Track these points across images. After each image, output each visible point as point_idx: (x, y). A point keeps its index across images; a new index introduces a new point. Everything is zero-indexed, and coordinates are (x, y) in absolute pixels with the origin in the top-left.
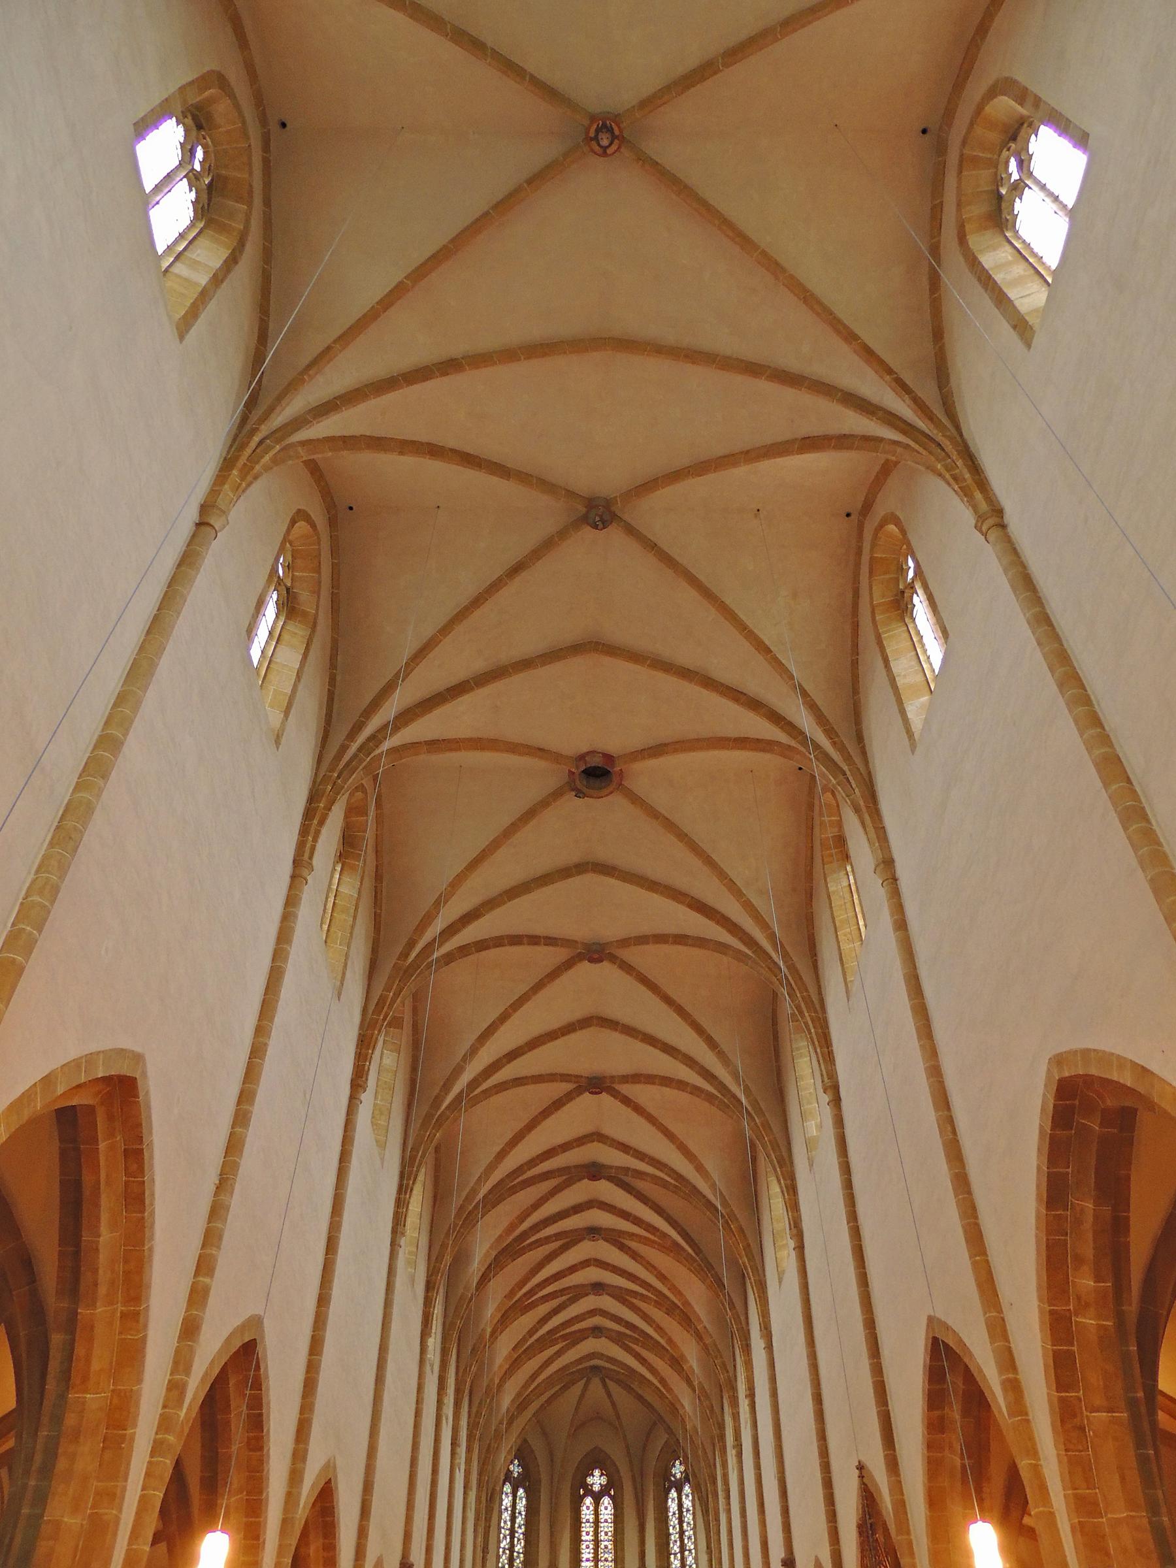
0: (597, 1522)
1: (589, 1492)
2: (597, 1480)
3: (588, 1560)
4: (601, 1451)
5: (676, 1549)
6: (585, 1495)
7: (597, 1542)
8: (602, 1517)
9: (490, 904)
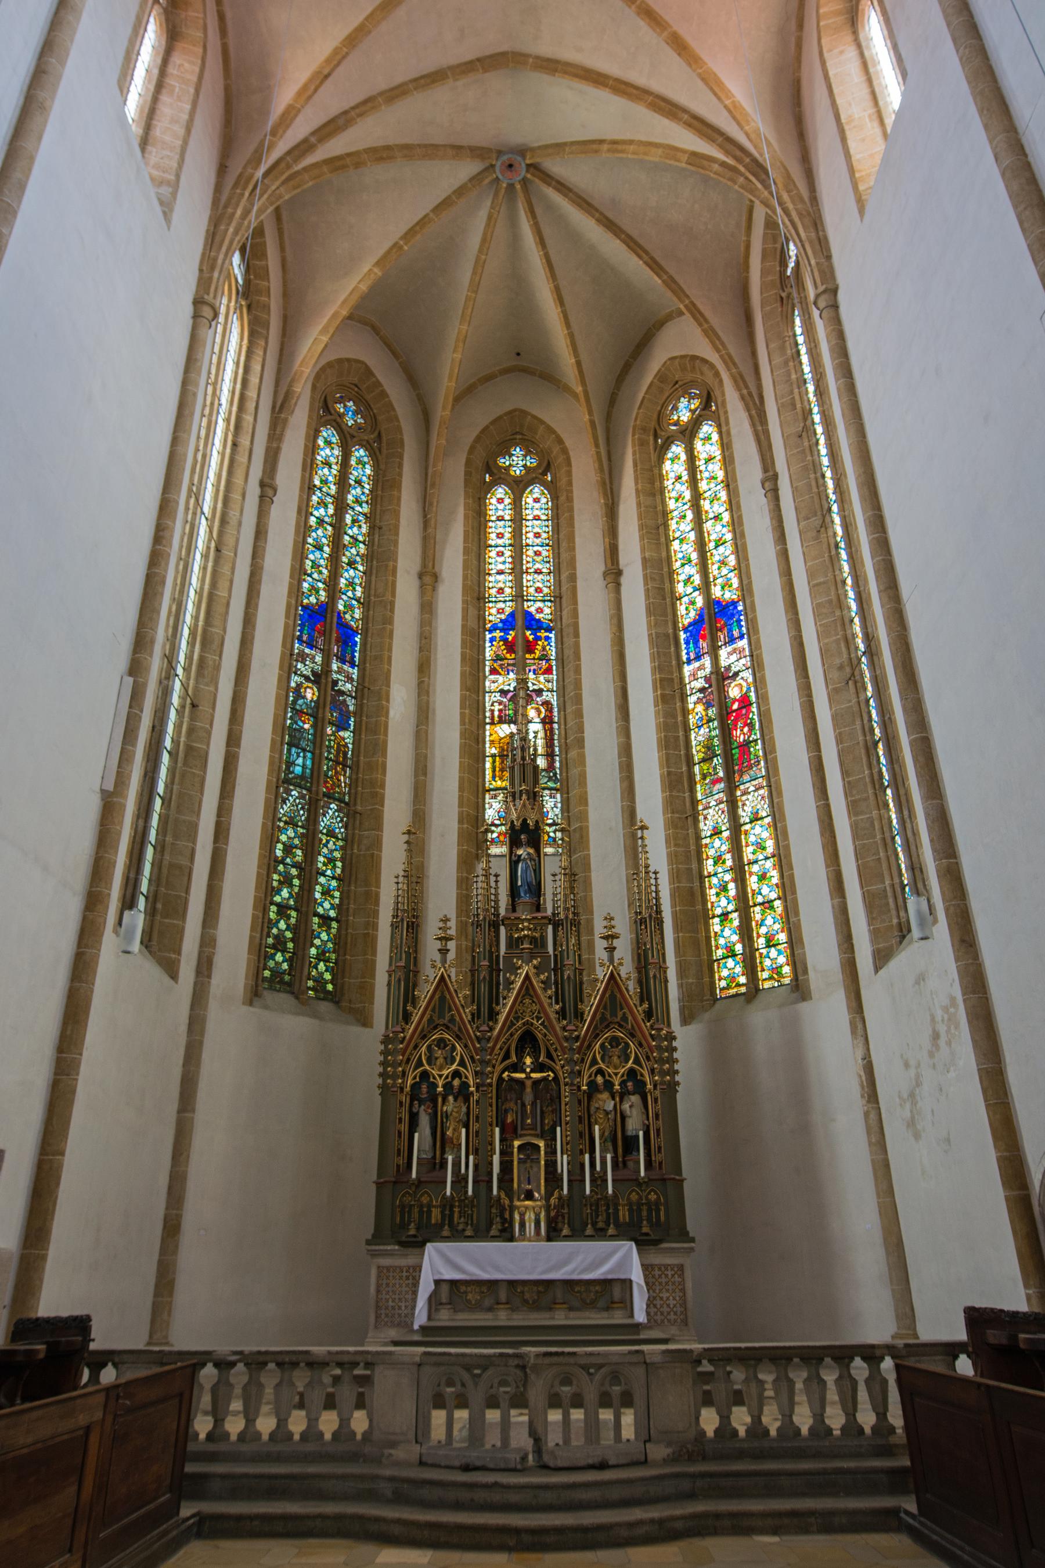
0: (518, 520)
1: (501, 477)
2: (517, 462)
3: (500, 572)
4: (524, 413)
5: (686, 526)
6: (496, 482)
7: (518, 547)
8: (528, 514)
9: (368, 105)
